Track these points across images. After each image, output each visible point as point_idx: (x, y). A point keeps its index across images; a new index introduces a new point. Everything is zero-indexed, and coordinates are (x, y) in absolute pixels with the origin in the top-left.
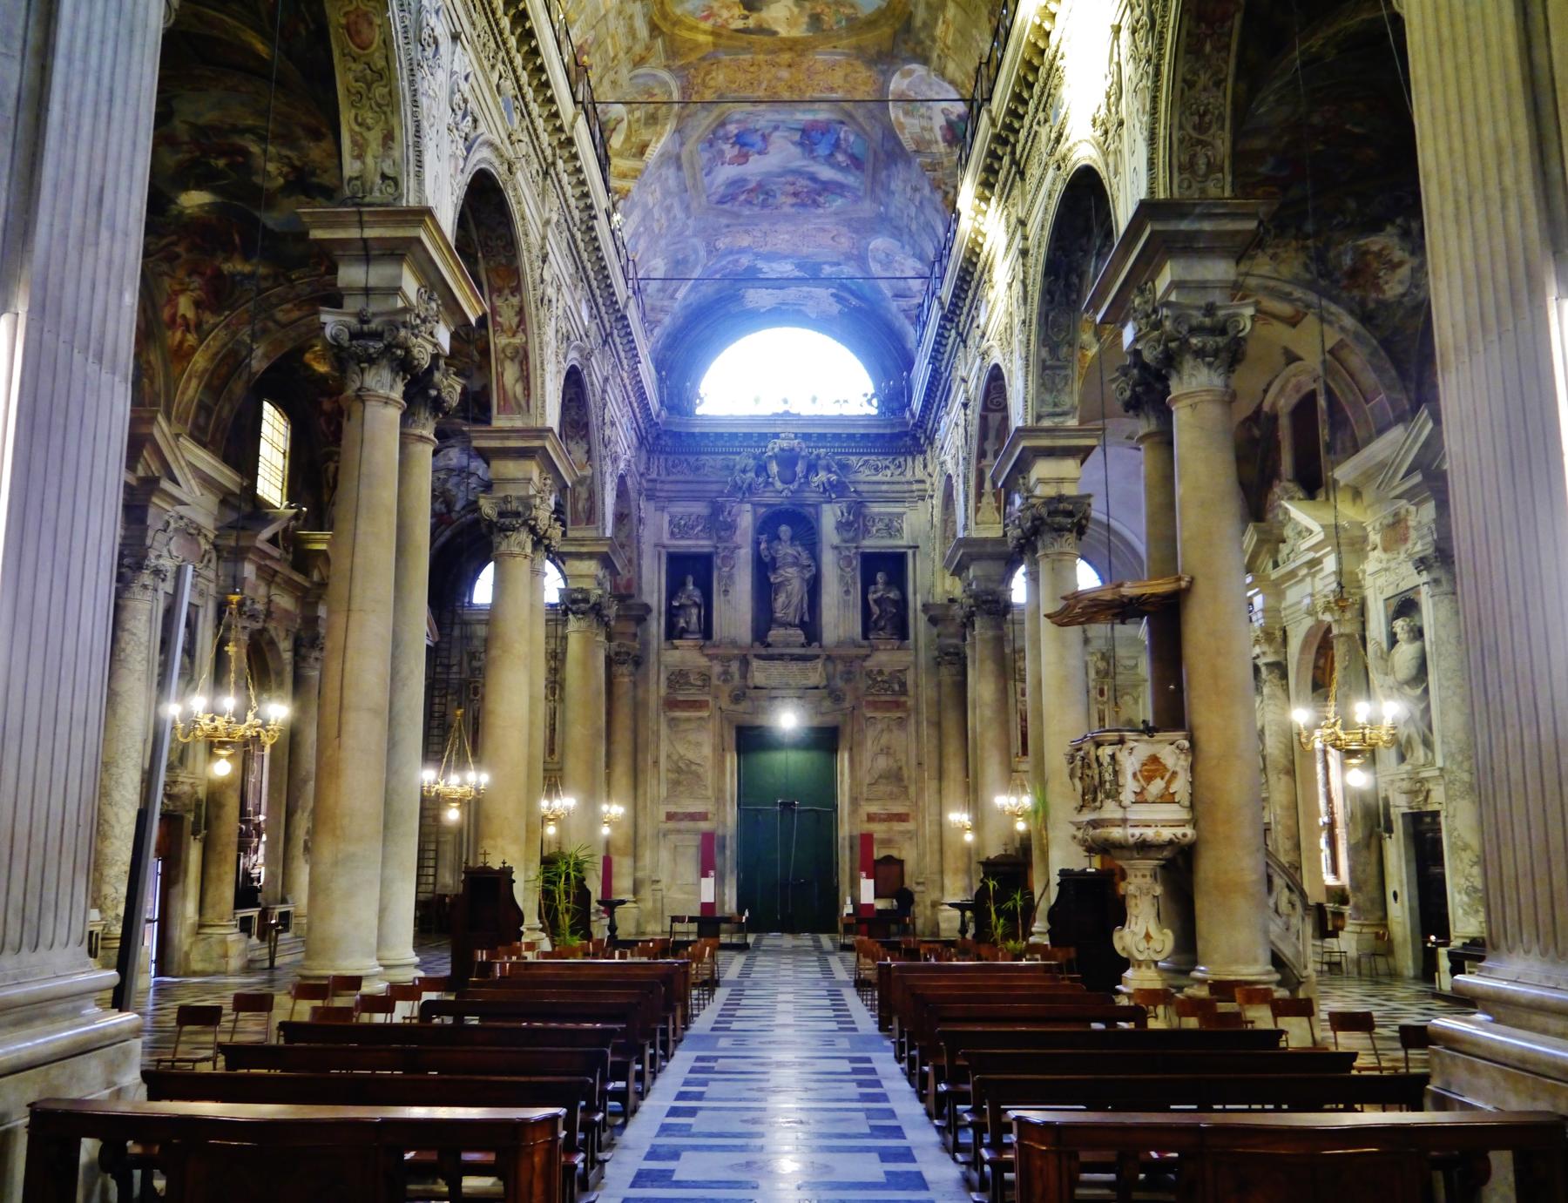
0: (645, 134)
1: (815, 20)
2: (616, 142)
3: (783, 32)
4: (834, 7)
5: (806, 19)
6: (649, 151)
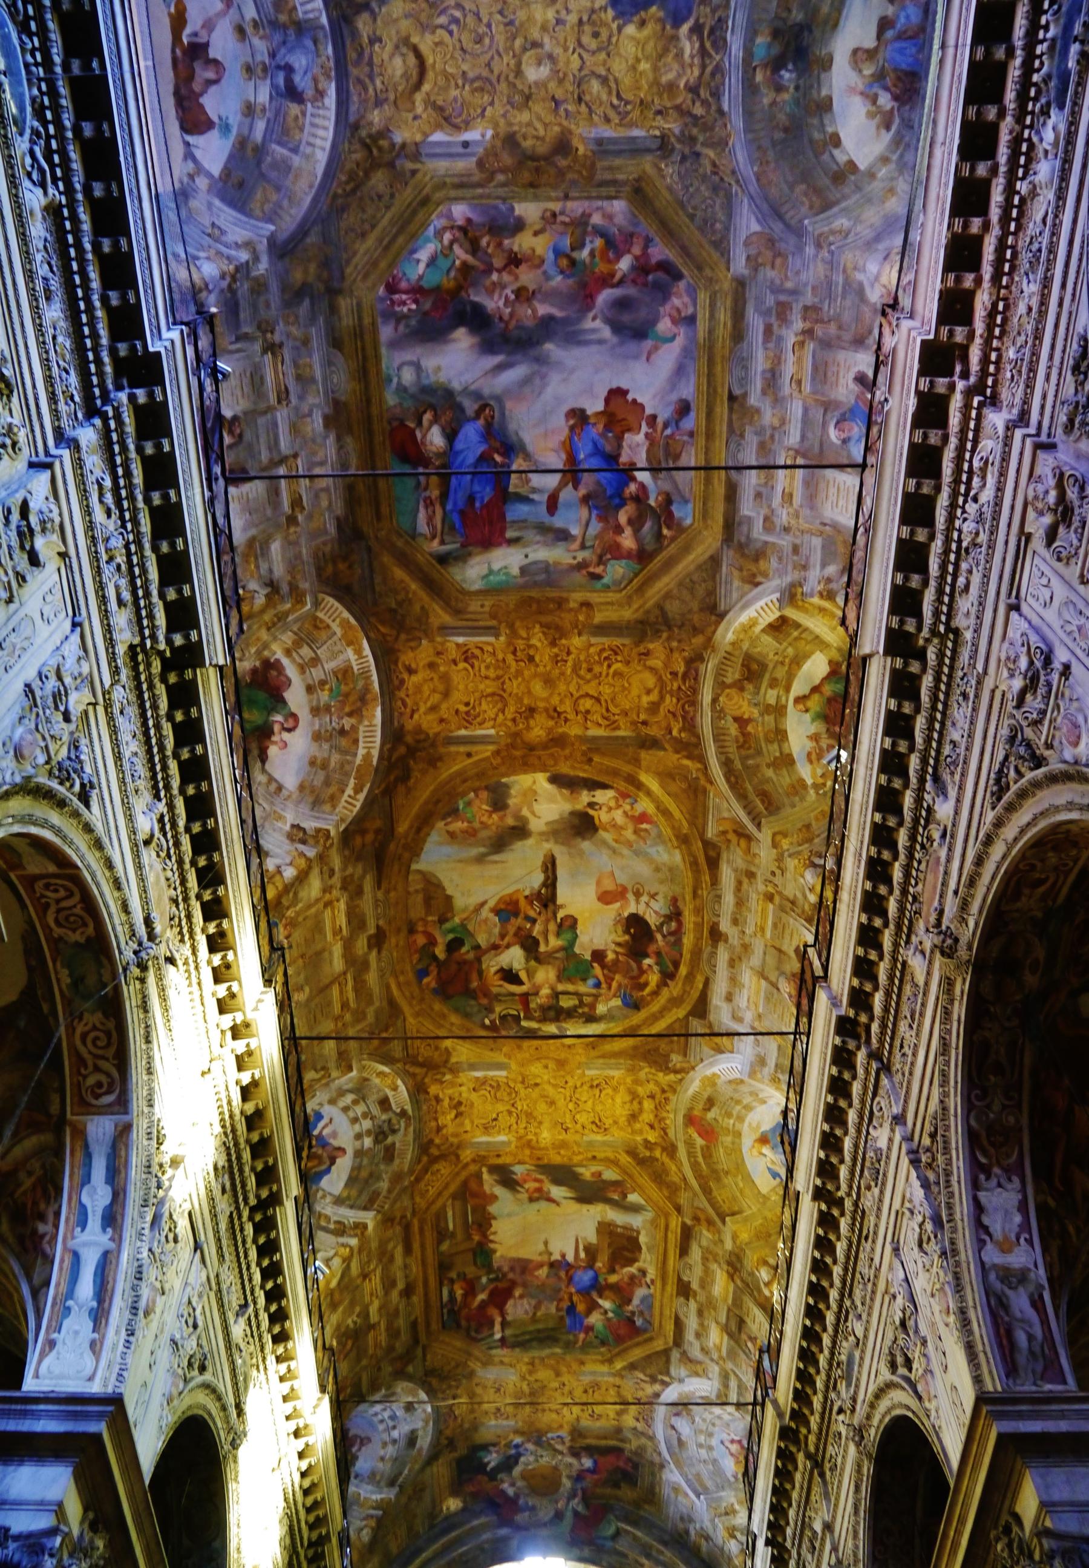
0: (768, 646)
1: (499, 801)
2: (817, 667)
3: (540, 781)
4: (477, 825)
5: (511, 802)
6: (772, 616)
